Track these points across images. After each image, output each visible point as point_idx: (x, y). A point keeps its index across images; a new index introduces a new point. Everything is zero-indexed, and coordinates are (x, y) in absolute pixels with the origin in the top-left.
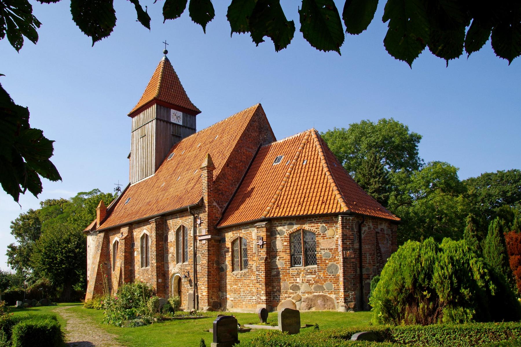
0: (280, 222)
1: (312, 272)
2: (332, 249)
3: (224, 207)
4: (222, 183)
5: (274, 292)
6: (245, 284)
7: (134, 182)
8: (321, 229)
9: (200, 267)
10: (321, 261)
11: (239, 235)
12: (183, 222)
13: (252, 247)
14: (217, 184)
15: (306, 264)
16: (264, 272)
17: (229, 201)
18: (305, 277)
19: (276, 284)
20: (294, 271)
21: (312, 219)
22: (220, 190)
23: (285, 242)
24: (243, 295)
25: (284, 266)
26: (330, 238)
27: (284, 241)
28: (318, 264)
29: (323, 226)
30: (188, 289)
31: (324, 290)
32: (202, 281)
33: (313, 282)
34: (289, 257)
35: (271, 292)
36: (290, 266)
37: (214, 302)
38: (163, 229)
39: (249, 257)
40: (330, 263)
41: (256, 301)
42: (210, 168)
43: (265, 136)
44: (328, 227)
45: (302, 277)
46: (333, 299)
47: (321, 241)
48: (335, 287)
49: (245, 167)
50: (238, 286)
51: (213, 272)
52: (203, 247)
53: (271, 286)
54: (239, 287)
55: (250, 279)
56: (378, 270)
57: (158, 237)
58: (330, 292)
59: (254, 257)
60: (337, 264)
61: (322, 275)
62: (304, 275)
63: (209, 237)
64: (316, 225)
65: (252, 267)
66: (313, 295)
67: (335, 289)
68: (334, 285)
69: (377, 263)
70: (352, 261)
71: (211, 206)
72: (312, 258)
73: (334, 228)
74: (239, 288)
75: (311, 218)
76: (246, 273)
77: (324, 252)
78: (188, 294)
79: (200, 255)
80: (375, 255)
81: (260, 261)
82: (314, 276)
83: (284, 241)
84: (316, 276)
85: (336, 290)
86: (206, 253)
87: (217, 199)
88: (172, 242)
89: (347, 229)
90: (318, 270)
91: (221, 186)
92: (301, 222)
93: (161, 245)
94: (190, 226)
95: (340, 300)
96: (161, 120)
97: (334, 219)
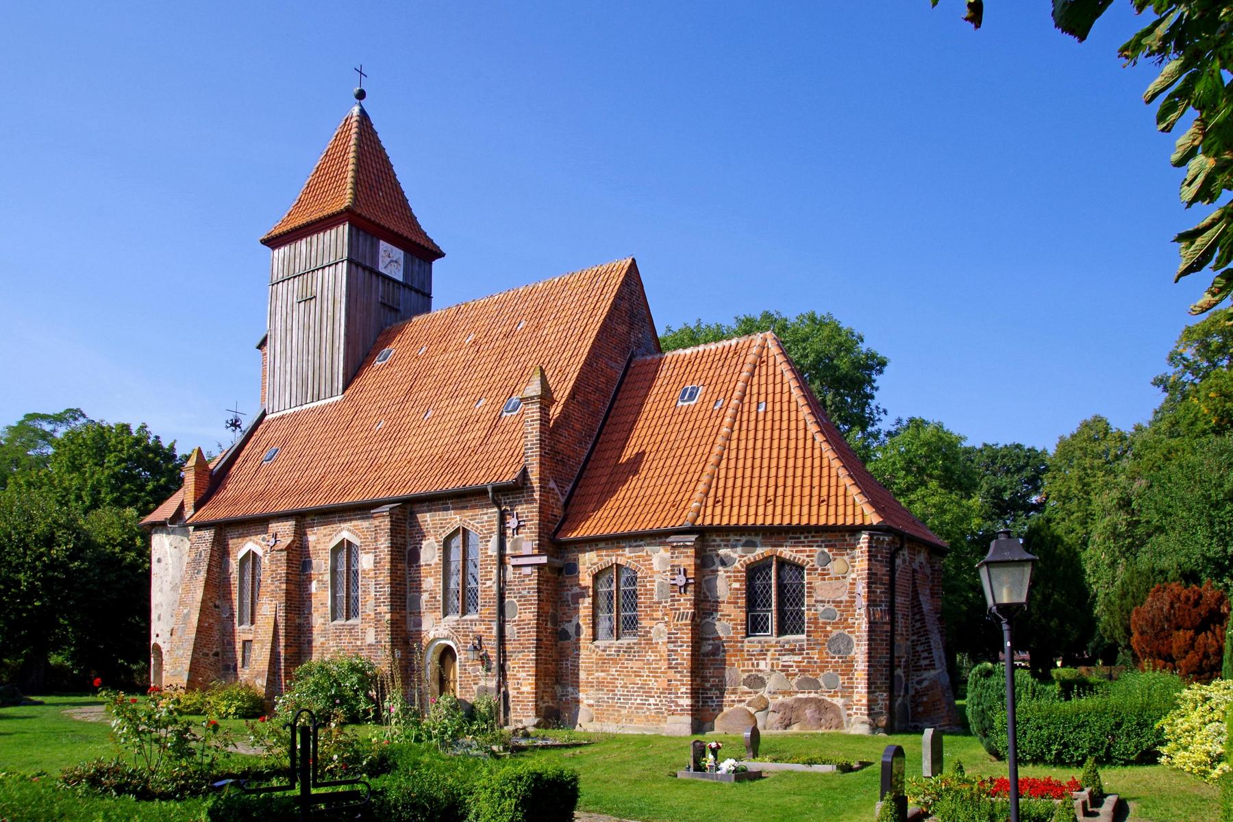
0: (725, 538)
1: (794, 650)
2: (841, 602)
3: (566, 492)
4: (562, 436)
5: (705, 689)
7: (276, 410)
8: (819, 559)
9: (515, 628)
10: (815, 627)
11: (617, 559)
12: (465, 521)
13: (653, 590)
15: (782, 631)
16: (687, 646)
17: (574, 479)
18: (778, 659)
19: (710, 673)
20: (754, 646)
21: (798, 535)
22: (559, 453)
23: (735, 581)
24: (620, 695)
25: (731, 635)
26: (837, 579)
27: (732, 579)
29: (823, 553)
30: (477, 676)
31: (820, 687)
32: (519, 659)
33: (797, 670)
34: (743, 615)
35: (699, 689)
36: (744, 635)
37: (547, 707)
38: (405, 534)
39: (642, 611)
40: (835, 632)
41: (656, 709)
42: (545, 399)
43: (640, 336)
45: (772, 659)
46: (839, 708)
47: (817, 584)
48: (844, 683)
49: (604, 403)
50: (609, 675)
51: (547, 640)
52: (523, 581)
54: (613, 675)
56: (913, 649)
58: (832, 693)
59: (657, 611)
60: (850, 635)
61: (816, 656)
62: (775, 655)
63: (544, 560)
64: (808, 549)
65: (650, 632)
66: (794, 697)
67: (843, 687)
68: (842, 679)
69: (913, 634)
71: (546, 488)
72: (794, 618)
73: (846, 558)
74: (611, 679)
75: (796, 533)
76: (632, 645)
77: (822, 609)
78: (475, 687)
79: (515, 600)
80: (910, 618)
81: (678, 620)
83: (732, 579)
84: (803, 658)
85: (845, 690)
86: (533, 596)
88: (430, 565)
89: (877, 561)
90: (807, 644)
92: (773, 540)
93: (400, 570)
94: (485, 532)
95: (854, 710)
96: (358, 265)
97: (847, 538)
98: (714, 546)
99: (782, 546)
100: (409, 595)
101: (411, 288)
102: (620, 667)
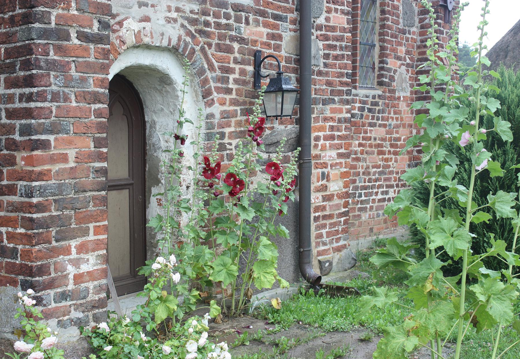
6: (372, 142)
32: (325, 119)
55: (385, 126)
76: (377, 100)
102: (364, 139)
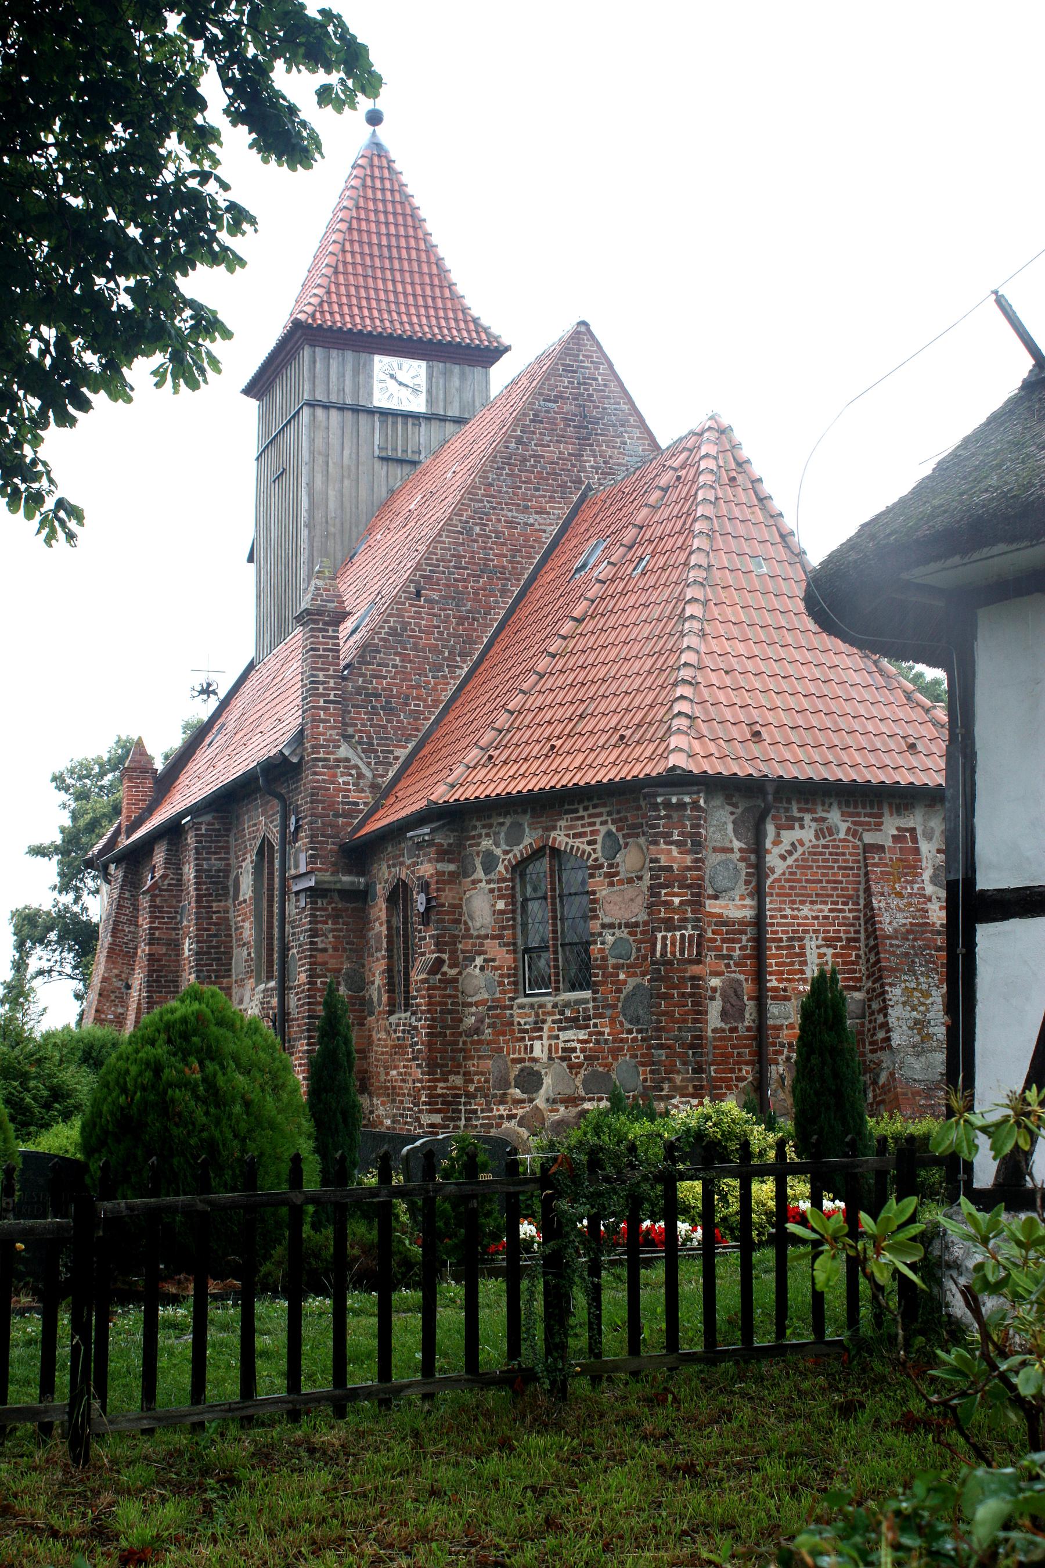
2: (636, 924)
3: (397, 758)
5: (470, 1096)
8: (603, 847)
14: (364, 675)
17: (420, 735)
22: (377, 696)
23: (500, 897)
25: (498, 995)
26: (630, 881)
28: (595, 983)
38: (228, 853)
40: (632, 982)
44: (624, 836)
45: (550, 1038)
47: (604, 893)
48: (645, 1080)
49: (504, 592)
53: (458, 1073)
57: (205, 883)
61: (607, 1030)
64: (588, 829)
70: (688, 975)
73: (642, 840)
75: (571, 803)
82: (582, 1035)
84: (590, 1034)
87: (361, 731)
89: (672, 843)
91: (385, 678)
98: (473, 837)
99: (554, 828)
100: (235, 952)
101: (443, 419)
